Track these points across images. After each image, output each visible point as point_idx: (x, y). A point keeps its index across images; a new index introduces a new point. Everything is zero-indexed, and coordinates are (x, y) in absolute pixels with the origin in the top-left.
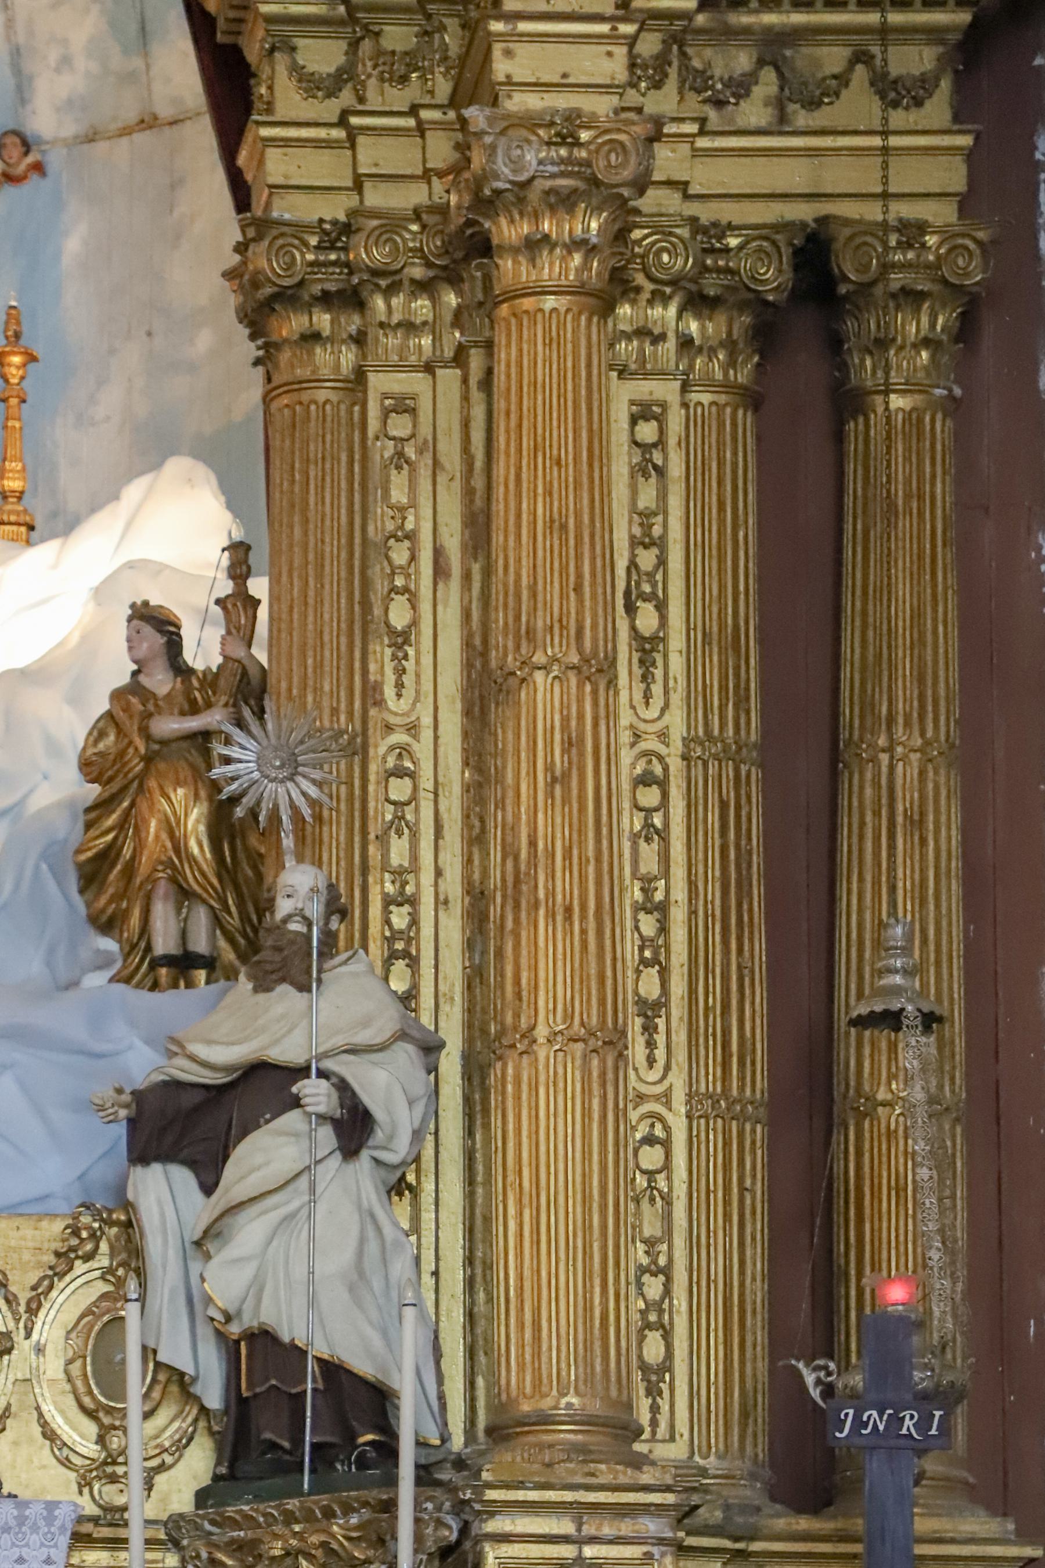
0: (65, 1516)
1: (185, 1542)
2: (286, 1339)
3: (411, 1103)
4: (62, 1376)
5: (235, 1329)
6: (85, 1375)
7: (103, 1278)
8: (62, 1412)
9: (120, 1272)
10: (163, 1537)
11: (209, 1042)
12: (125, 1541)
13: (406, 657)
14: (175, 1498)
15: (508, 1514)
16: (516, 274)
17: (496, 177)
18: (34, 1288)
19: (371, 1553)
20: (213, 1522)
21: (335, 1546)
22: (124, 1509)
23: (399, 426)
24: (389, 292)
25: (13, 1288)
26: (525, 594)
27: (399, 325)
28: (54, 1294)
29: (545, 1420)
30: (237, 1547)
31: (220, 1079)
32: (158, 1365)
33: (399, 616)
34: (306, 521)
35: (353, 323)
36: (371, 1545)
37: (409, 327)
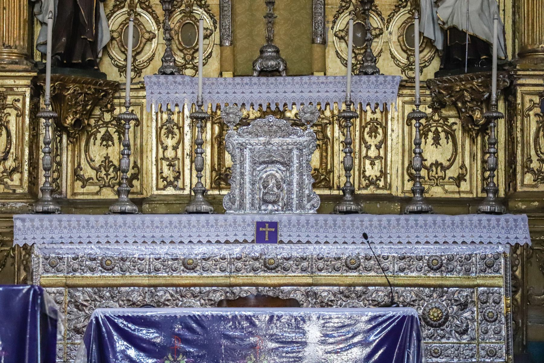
0: (397, 80)
1: (432, 87)
2: (461, 29)
4: (397, 40)
5: (446, 27)
6: (403, 40)
7: (408, 13)
8: (397, 51)
9: (413, 11)
10: (425, 85)
12: (414, 87)
14: (429, 75)
15: (524, 78)
18: (389, 16)
19: (485, 90)
20: (439, 81)
21: (474, 88)
22: (414, 78)
25: (383, 16)
28: (395, 17)
29: (536, 51)
30: (445, 89)
32: (424, 37)
36: (485, 87)
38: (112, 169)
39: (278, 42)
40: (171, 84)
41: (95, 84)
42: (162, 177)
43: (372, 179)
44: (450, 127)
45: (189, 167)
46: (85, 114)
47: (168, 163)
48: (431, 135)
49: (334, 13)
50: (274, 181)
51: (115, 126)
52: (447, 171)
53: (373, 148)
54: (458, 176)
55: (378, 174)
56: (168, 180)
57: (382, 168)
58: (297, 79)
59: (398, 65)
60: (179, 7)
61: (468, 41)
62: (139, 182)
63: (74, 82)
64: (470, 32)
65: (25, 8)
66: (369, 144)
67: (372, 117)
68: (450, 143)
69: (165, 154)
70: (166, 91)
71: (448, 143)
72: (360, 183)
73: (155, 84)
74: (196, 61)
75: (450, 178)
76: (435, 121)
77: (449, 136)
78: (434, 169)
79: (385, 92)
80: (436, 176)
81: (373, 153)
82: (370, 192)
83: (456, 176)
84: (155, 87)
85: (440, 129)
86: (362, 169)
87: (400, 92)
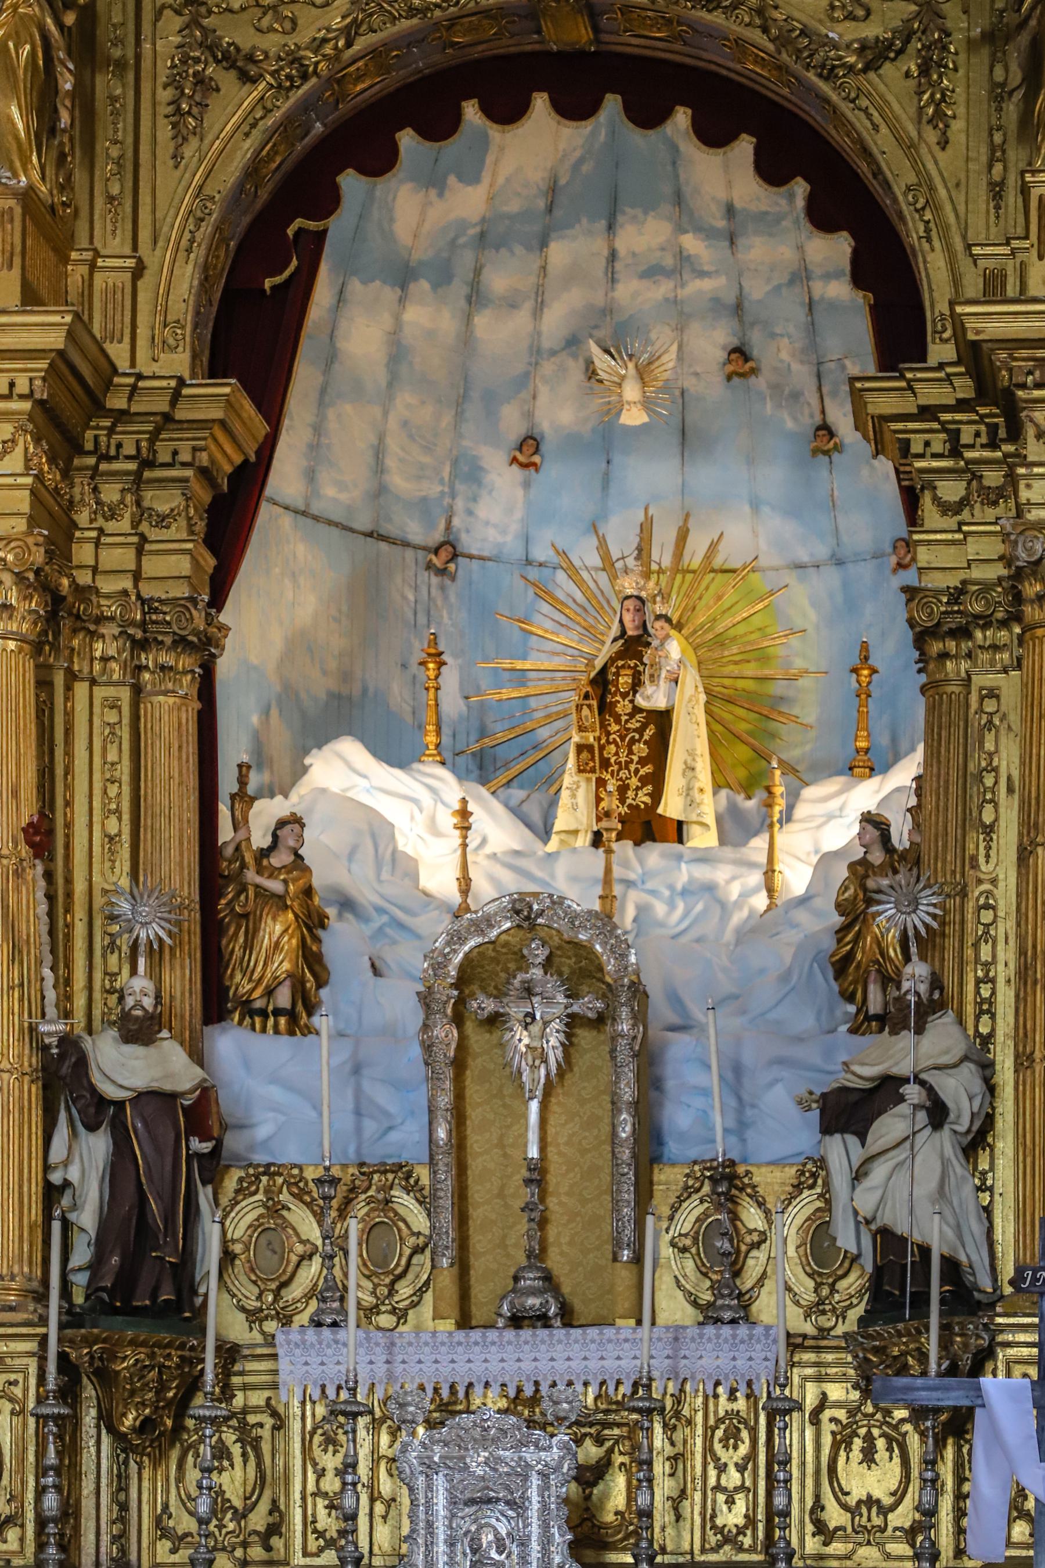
3: (971, 1099)
11: (863, 1064)
13: (991, 839)
16: (1033, 616)
17: (1018, 559)
23: (990, 706)
24: (984, 627)
26: (1033, 802)
27: (990, 646)
31: (868, 1085)
33: (988, 817)
34: (939, 762)
35: (966, 646)
37: (995, 648)
38: (229, 1515)
39: (555, 1261)
40: (329, 1346)
41: (182, 1346)
42: (315, 1531)
43: (730, 1531)
44: (895, 1427)
45: (367, 1511)
46: (163, 1408)
47: (327, 1502)
48: (858, 1443)
49: (673, 1200)
50: (491, 1537)
51: (235, 1429)
52: (890, 1516)
53: (330, 1474)
54: (911, 1526)
55: (741, 1521)
56: (328, 1536)
57: (748, 1510)
58: (593, 1332)
59: (797, 1303)
60: (365, 1191)
61: (913, 1255)
62: (282, 1540)
63: (134, 1343)
64: (917, 1237)
65: (34, 1198)
66: (723, 1460)
67: (729, 1408)
68: (897, 1460)
69: (322, 1484)
70: (319, 1360)
71: (891, 1458)
72: (704, 1540)
73: (297, 1345)
74: (396, 1299)
75: (896, 1529)
76: (866, 1415)
77: (895, 1445)
78: (864, 1510)
79: (750, 1359)
80: (869, 1525)
81: (733, 1478)
82: (724, 1559)
83: (907, 1525)
84: (298, 1352)
85: (876, 1432)
86: (709, 1511)
87: (796, 1359)
